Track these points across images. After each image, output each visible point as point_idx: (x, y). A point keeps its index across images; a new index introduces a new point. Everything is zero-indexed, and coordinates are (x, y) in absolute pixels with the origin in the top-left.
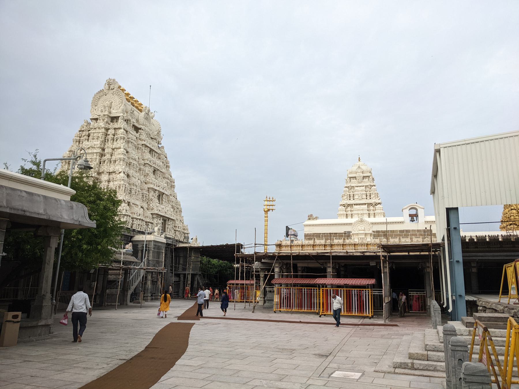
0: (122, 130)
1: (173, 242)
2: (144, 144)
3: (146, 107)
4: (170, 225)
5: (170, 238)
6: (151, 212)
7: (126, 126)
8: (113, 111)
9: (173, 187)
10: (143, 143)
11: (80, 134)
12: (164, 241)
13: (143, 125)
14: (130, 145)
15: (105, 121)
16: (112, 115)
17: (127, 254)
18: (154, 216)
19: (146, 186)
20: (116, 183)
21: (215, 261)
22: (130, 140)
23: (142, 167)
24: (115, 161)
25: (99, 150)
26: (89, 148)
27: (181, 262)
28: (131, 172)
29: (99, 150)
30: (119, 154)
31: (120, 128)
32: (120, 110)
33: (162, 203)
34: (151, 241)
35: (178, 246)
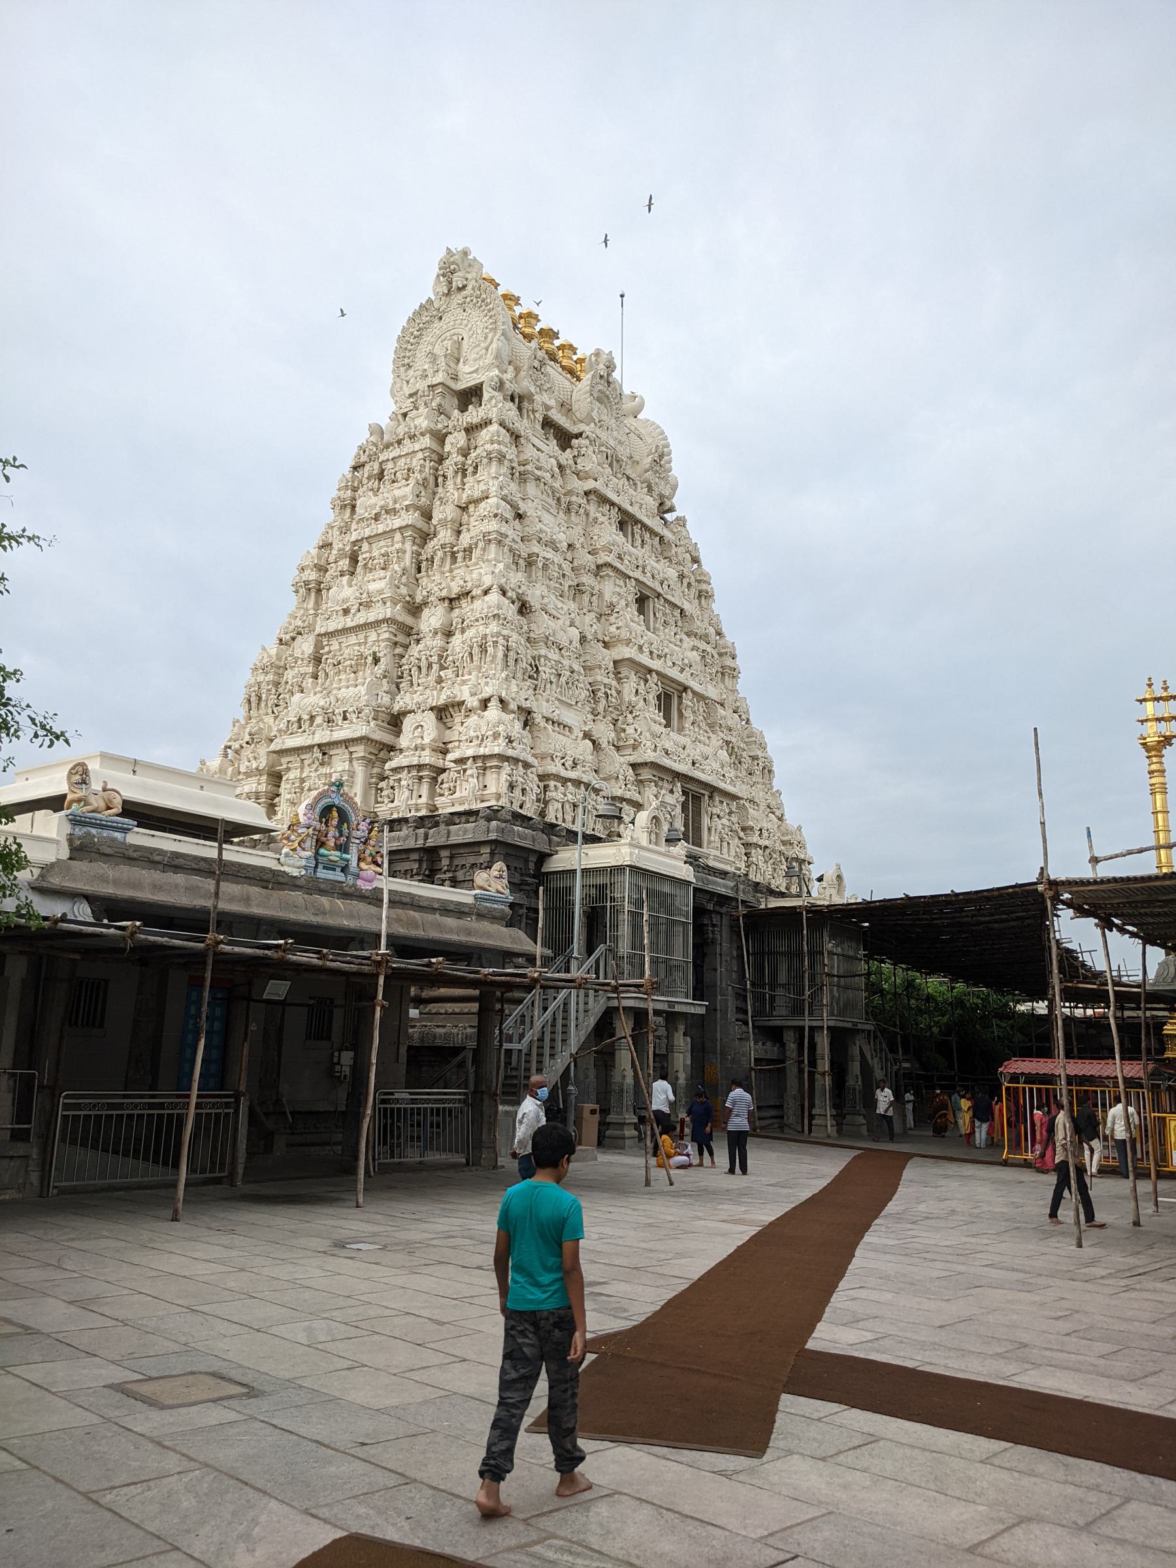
0: (494, 428)
1: (736, 889)
2: (594, 492)
3: (598, 354)
4: (717, 821)
5: (724, 874)
6: (632, 759)
7: (514, 412)
8: (464, 369)
9: (728, 673)
10: (590, 485)
11: (354, 477)
12: (686, 872)
13: (589, 420)
14: (531, 489)
15: (434, 404)
16: (461, 386)
17: (481, 916)
18: (646, 774)
19: (606, 657)
20: (470, 633)
21: (934, 984)
22: (528, 467)
23: (587, 579)
24: (469, 551)
25: (411, 518)
26: (377, 518)
27: (783, 978)
28: (536, 594)
29: (411, 518)
30: (478, 525)
31: (487, 423)
32: (489, 359)
33: (681, 730)
34: (620, 869)
35: (763, 906)
